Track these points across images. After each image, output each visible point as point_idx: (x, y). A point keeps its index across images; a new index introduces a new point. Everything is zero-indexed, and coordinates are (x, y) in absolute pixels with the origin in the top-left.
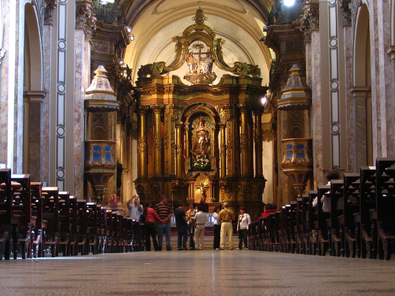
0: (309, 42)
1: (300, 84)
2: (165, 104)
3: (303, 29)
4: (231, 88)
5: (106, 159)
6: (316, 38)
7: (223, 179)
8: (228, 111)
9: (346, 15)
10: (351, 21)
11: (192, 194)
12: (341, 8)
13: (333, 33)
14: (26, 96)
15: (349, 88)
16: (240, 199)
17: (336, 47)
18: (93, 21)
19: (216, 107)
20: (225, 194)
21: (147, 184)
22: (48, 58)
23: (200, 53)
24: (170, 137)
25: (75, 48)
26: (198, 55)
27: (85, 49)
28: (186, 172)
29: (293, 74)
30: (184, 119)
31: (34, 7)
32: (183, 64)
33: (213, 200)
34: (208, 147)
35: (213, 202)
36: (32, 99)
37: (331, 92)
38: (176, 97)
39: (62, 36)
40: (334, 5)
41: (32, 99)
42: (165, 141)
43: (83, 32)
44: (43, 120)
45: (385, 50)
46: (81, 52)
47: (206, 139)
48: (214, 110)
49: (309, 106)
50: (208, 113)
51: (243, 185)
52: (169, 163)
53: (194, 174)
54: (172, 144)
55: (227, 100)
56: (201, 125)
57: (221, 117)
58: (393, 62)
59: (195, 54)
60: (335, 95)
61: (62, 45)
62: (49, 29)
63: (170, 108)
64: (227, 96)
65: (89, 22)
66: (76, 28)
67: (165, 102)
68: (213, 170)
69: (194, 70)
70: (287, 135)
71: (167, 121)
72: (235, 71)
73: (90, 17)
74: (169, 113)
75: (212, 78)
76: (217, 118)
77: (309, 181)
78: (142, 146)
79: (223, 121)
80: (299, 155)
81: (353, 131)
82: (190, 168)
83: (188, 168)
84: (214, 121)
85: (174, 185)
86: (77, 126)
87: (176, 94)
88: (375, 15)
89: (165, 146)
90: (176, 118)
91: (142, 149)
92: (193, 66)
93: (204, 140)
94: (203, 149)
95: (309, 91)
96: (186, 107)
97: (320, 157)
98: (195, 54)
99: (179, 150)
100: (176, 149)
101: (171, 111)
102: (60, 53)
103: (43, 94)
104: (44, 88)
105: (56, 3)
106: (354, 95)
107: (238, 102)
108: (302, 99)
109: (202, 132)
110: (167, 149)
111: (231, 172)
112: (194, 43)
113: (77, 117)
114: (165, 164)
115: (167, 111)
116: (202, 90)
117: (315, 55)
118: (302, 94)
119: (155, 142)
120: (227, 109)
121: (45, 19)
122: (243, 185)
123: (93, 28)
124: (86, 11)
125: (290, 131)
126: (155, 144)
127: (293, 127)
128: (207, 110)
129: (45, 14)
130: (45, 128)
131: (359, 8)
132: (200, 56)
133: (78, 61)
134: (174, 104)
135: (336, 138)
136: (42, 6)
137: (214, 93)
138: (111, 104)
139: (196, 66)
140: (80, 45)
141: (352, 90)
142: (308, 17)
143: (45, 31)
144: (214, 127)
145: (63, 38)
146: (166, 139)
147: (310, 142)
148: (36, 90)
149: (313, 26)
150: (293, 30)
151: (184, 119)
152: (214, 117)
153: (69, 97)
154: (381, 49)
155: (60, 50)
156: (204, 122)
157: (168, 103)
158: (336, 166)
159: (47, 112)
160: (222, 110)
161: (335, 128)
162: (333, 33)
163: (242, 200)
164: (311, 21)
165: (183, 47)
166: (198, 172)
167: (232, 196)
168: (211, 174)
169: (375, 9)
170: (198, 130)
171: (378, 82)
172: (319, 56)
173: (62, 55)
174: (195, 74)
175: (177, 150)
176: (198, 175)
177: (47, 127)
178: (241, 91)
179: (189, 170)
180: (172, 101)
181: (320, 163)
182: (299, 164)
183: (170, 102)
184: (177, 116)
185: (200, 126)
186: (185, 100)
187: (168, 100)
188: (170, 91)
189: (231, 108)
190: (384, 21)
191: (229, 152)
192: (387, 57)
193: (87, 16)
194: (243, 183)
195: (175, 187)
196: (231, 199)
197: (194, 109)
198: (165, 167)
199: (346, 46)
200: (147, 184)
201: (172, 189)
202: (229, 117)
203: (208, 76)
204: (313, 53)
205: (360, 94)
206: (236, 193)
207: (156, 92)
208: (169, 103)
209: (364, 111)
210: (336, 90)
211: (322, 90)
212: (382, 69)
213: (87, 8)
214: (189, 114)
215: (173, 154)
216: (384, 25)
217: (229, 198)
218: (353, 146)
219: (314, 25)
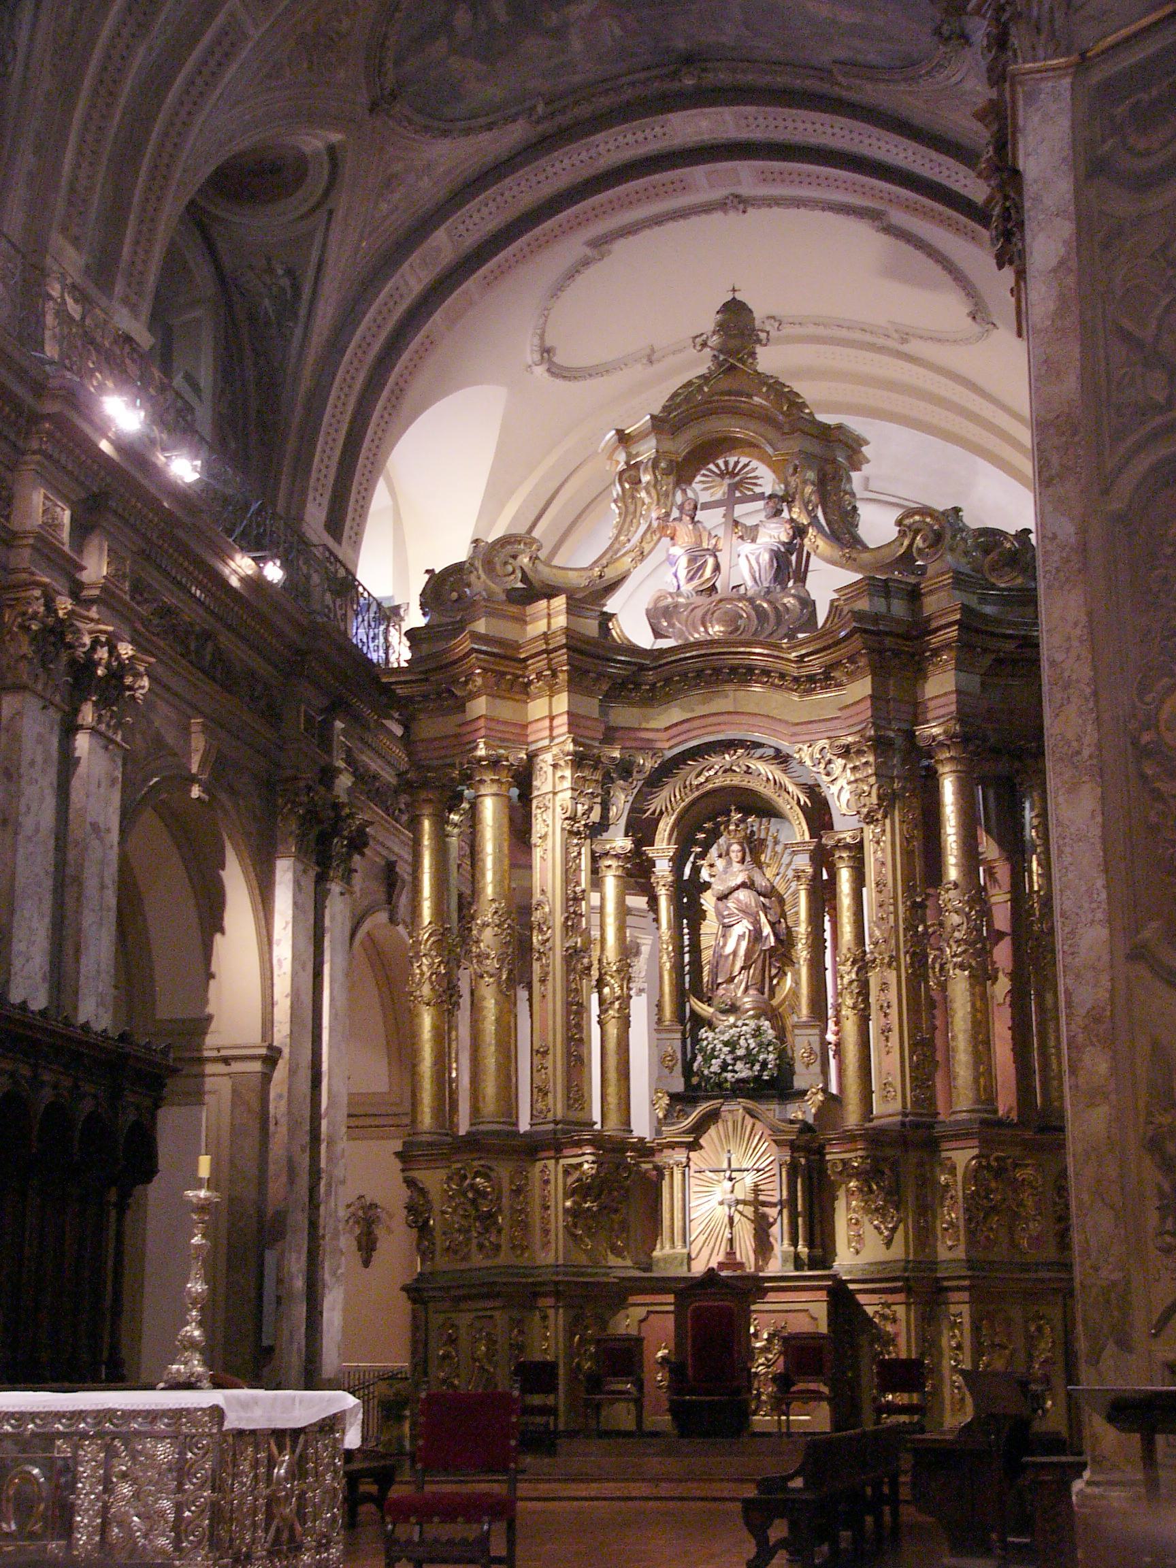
2: (533, 747)
4: (886, 640)
7: (849, 1138)
8: (867, 763)
11: (678, 1224)
16: (950, 1250)
20: (866, 1220)
24: (559, 919)
26: (722, 510)
32: (642, 556)
33: (797, 1256)
34: (782, 974)
35: (798, 1267)
38: (591, 706)
42: (536, 938)
50: (768, 791)
51: (960, 1172)
52: (550, 1057)
54: (573, 956)
55: (862, 706)
56: (742, 861)
63: (555, 766)
64: (862, 687)
67: (538, 735)
69: (696, 582)
70: (1083, 548)
71: (543, 837)
74: (555, 793)
75: (787, 609)
76: (818, 813)
78: (422, 974)
79: (845, 824)
84: (798, 830)
85: (576, 1175)
87: (590, 693)
89: (536, 966)
90: (595, 816)
91: (426, 990)
92: (692, 560)
93: (756, 936)
96: (647, 763)
98: (706, 506)
99: (612, 989)
101: (562, 777)
107: (917, 714)
110: (543, 981)
111: (894, 1098)
115: (543, 783)
116: (734, 669)
119: (478, 942)
120: (860, 752)
122: (960, 1172)
125: (1116, 506)
126: (478, 956)
128: (763, 774)
134: (575, 742)
137: (796, 680)
139: (711, 561)
144: (803, 862)
146: (541, 931)
151: (641, 829)
152: (804, 809)
156: (754, 849)
157: (546, 742)
163: (960, 1253)
165: (646, 478)
167: (899, 1236)
174: (702, 600)
175: (606, 990)
176: (712, 1117)
178: (936, 652)
180: (565, 729)
183: (555, 733)
184: (597, 809)
185: (736, 867)
186: (644, 725)
187: (547, 723)
188: (554, 675)
189: (880, 745)
191: (884, 987)
194: (962, 1157)
195: (582, 1190)
196: (897, 1251)
197: (698, 775)
201: (566, 1197)
202: (874, 800)
203: (769, 602)
206: (925, 1211)
207: (479, 681)
208: (552, 738)
214: (670, 802)
217: (889, 1243)
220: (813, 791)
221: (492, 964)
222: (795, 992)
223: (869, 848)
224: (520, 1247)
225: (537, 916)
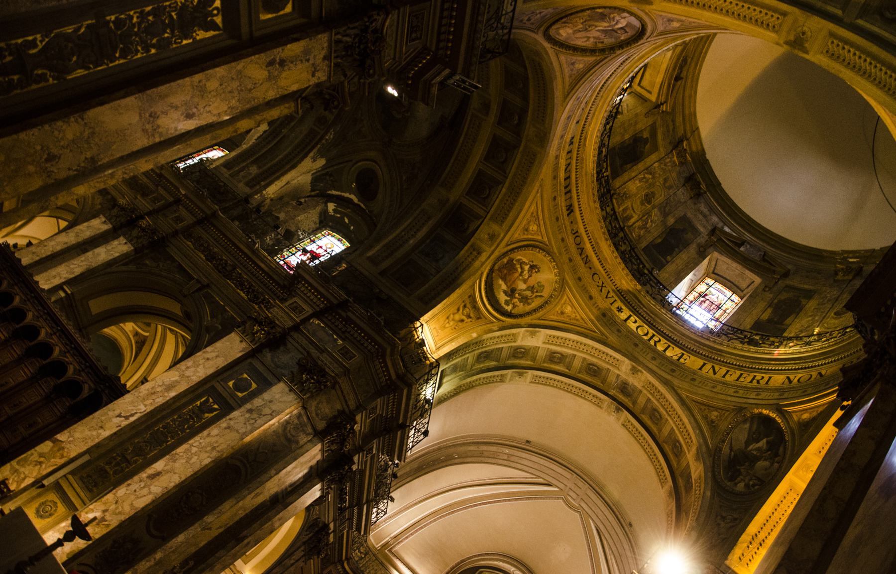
127: (238, 464)
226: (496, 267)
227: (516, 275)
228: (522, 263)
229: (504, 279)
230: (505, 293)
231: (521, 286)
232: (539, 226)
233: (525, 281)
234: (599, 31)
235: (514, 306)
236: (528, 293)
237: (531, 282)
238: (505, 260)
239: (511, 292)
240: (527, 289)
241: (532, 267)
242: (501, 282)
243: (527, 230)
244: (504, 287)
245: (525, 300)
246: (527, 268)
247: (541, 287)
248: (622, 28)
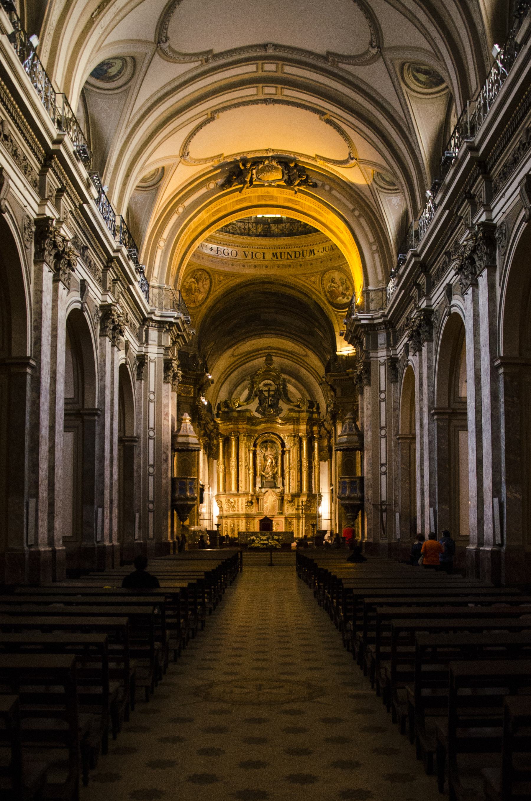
0: (362, 393)
1: (354, 430)
3: (357, 382)
5: (190, 492)
6: (367, 391)
9: (394, 372)
10: (397, 377)
12: (390, 366)
13: (383, 388)
14: (120, 440)
15: (396, 435)
17: (385, 400)
18: (179, 375)
19: (282, 436)
21: (225, 499)
22: (140, 408)
23: (269, 391)
24: (244, 461)
25: (163, 399)
27: (172, 398)
28: (257, 489)
29: (348, 421)
30: (255, 445)
31: (128, 366)
36: (126, 444)
37: (380, 438)
39: (152, 389)
40: (384, 364)
41: (126, 444)
43: (170, 384)
44: (136, 461)
45: (430, 409)
46: (168, 403)
47: (274, 462)
48: (280, 438)
49: (361, 449)
50: (274, 440)
53: (264, 490)
57: (286, 444)
58: (436, 421)
59: (265, 391)
60: (383, 441)
61: (152, 397)
62: (141, 383)
65: (175, 376)
66: (164, 382)
68: (279, 488)
72: (298, 406)
73: (175, 372)
76: (283, 445)
77: (360, 512)
80: (353, 490)
81: (399, 471)
82: (260, 486)
83: (259, 485)
86: (165, 465)
88: (421, 379)
93: (272, 462)
94: (271, 470)
95: (361, 436)
96: (257, 435)
97: (370, 493)
98: (265, 391)
100: (249, 470)
102: (150, 403)
103: (137, 439)
104: (137, 434)
105: (146, 361)
106: (400, 441)
108: (356, 443)
109: (271, 457)
112: (266, 382)
113: (165, 458)
114: (240, 482)
117: (367, 406)
118: (356, 438)
121: (137, 374)
123: (179, 380)
124: (173, 367)
129: (137, 370)
130: (138, 468)
131: (406, 369)
132: (269, 393)
133: (166, 410)
135: (384, 477)
136: (134, 364)
138: (194, 446)
140: (167, 396)
141: (398, 437)
142: (361, 373)
143: (136, 386)
144: (280, 452)
145: (153, 390)
147: (362, 479)
148: (129, 435)
149: (365, 381)
150: (347, 377)
153: (158, 441)
154: (425, 409)
155: (150, 401)
156: (271, 447)
158: (383, 501)
159: (140, 454)
160: (286, 438)
161: (383, 469)
162: (383, 388)
164: (364, 377)
166: (267, 489)
168: (278, 490)
169: (421, 374)
170: (266, 455)
171: (422, 437)
172: (370, 407)
173: (152, 405)
176: (267, 491)
177: (139, 466)
179: (260, 488)
181: (370, 498)
182: (352, 497)
190: (428, 386)
192: (430, 417)
193: (173, 371)
194: (304, 499)
198: (240, 485)
199: (394, 399)
200: (225, 499)
204: (365, 401)
205: (405, 441)
209: (408, 455)
210: (385, 436)
211: (372, 436)
212: (426, 427)
213: (173, 365)
214: (259, 441)
215: (246, 474)
216: (428, 389)
218: (399, 484)
219: (366, 380)
220: (282, 440)
221: (234, 467)
222: (277, 472)
223: (291, 451)
224: (238, 511)
225: (240, 460)
226: (331, 300)
227: (336, 291)
228: (330, 287)
229: (337, 297)
230: (343, 298)
231: (341, 289)
232: (312, 276)
233: (339, 287)
234: (198, 285)
235: (349, 295)
236: (344, 286)
237: (339, 283)
238: (328, 295)
239: (344, 295)
240: (342, 286)
241: (332, 282)
242: (338, 299)
243: (314, 282)
244: (340, 298)
245: (347, 289)
246: (333, 284)
247: (341, 279)
248: (194, 278)
